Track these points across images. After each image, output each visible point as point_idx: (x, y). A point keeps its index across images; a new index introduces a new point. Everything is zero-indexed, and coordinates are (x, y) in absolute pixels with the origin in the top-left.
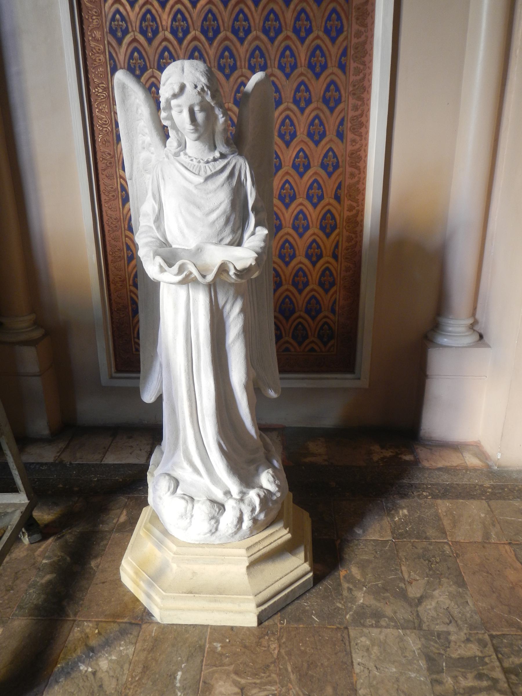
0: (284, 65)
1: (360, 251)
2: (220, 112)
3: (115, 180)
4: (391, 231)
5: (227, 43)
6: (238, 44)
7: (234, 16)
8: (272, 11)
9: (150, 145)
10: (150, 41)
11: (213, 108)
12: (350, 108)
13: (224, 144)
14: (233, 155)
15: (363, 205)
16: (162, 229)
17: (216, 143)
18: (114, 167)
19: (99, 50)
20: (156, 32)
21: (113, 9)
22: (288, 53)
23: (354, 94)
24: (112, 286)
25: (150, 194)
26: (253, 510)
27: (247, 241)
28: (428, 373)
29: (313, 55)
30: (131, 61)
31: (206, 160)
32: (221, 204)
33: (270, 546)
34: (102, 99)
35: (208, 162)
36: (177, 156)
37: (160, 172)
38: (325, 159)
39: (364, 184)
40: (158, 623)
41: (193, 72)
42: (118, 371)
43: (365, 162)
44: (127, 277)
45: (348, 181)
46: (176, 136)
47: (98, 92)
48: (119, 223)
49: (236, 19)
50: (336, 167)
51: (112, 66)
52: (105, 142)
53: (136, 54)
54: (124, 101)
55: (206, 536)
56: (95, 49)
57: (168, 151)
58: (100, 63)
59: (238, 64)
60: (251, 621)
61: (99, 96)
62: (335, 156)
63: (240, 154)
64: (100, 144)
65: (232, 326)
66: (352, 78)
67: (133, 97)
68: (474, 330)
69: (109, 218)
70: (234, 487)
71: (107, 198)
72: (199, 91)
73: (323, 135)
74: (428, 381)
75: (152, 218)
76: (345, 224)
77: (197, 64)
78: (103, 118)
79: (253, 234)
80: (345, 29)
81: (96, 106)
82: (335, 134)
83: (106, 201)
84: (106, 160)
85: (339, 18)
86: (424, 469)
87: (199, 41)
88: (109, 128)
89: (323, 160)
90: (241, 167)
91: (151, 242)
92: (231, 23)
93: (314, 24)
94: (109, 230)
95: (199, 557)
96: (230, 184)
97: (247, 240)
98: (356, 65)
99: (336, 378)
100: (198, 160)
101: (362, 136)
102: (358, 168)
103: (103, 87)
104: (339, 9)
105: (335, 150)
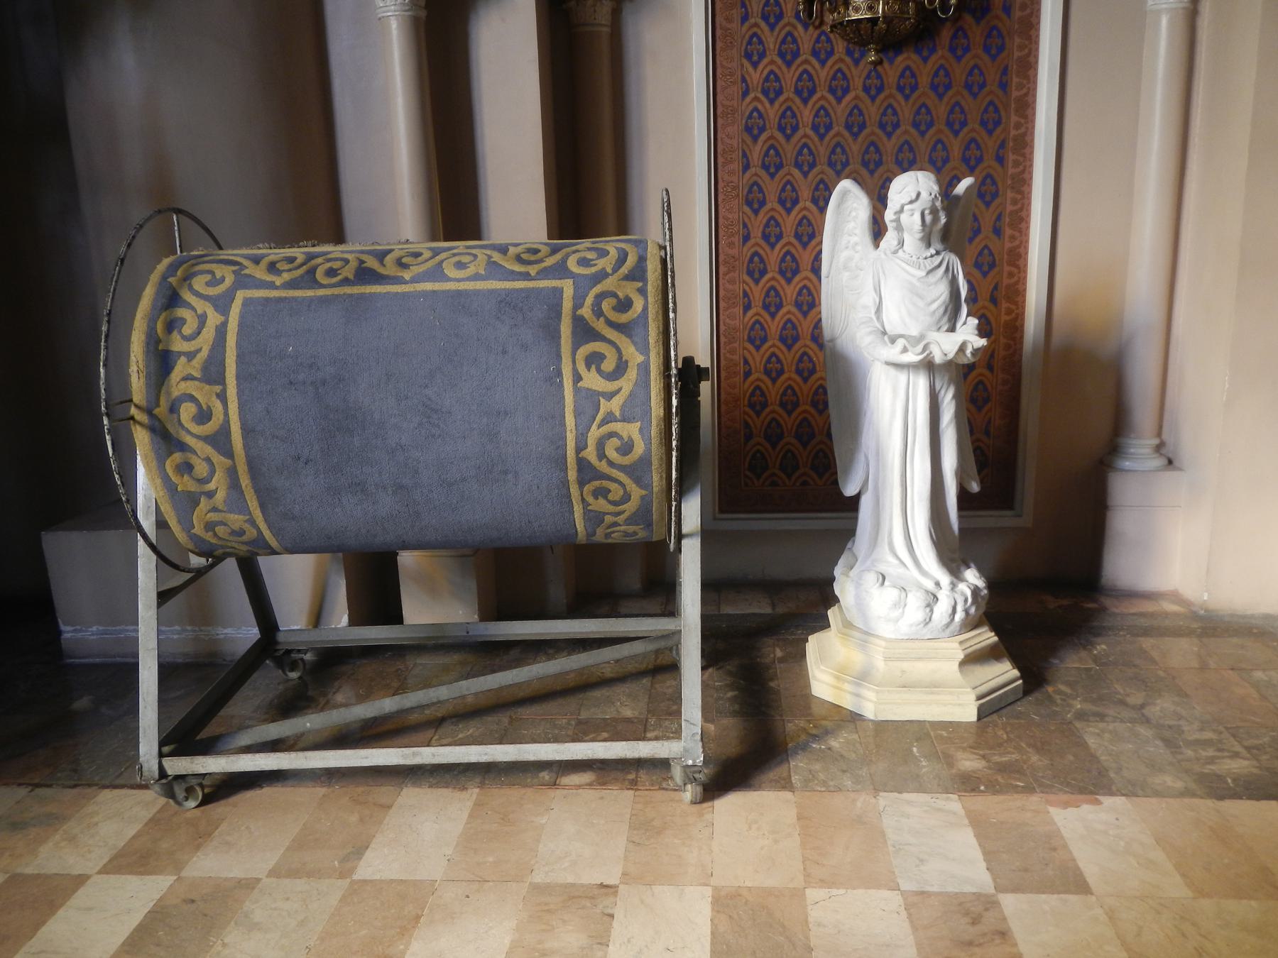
1: (1020, 360)
6: (885, 139)
7: (881, 111)
8: (924, 105)
9: (856, 244)
10: (788, 138)
12: (1008, 202)
15: (1024, 308)
17: (932, 241)
18: (737, 271)
21: (750, 108)
22: (939, 146)
23: (1013, 188)
24: (723, 408)
26: (966, 600)
28: (1110, 503)
29: (967, 148)
31: (924, 256)
33: (981, 640)
35: (926, 258)
39: (1025, 284)
40: (872, 721)
41: (927, 181)
42: (721, 511)
43: (1026, 260)
44: (742, 396)
45: (1006, 281)
48: (738, 334)
49: (884, 114)
50: (992, 265)
51: (744, 164)
55: (918, 628)
59: (884, 158)
62: (991, 254)
63: (950, 251)
65: (945, 412)
66: (1011, 171)
68: (1161, 454)
70: (945, 578)
74: (1110, 514)
75: (873, 311)
79: (965, 323)
80: (1004, 121)
82: (991, 230)
85: (997, 110)
87: (842, 136)
89: (977, 258)
92: (878, 119)
93: (969, 116)
95: (911, 651)
98: (1015, 157)
99: (991, 516)
102: (1018, 267)
104: (997, 102)
105: (991, 248)
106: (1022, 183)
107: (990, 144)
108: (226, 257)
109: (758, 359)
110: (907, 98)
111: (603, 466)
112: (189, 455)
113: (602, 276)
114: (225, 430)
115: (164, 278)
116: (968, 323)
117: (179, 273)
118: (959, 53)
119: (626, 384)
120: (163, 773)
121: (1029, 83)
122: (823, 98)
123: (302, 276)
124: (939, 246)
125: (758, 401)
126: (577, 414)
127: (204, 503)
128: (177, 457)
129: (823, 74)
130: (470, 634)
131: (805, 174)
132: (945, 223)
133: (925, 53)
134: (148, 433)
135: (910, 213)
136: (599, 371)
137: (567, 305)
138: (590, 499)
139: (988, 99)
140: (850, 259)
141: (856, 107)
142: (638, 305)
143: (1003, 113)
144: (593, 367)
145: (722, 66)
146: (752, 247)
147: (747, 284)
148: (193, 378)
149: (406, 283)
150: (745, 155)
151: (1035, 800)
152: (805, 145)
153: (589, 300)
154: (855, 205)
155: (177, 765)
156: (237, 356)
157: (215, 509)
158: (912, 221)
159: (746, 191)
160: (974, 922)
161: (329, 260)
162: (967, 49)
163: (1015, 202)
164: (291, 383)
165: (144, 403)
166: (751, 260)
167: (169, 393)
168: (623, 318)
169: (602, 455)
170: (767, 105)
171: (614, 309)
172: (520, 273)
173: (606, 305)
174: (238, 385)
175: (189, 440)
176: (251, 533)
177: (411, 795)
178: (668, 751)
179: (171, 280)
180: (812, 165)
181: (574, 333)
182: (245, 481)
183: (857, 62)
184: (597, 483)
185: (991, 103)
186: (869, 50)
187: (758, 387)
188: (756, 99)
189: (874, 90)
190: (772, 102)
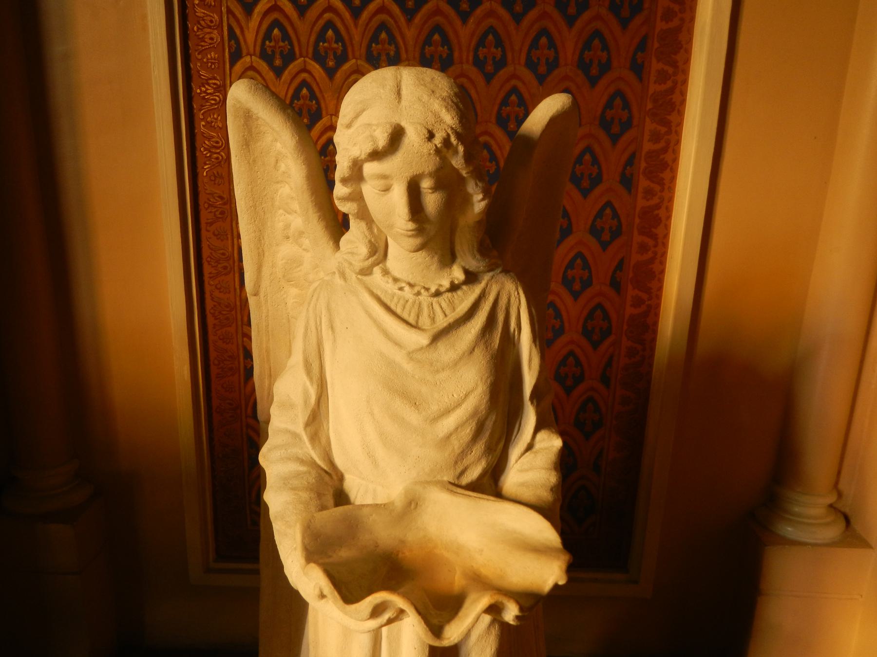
0: (536, 61)
2: (479, 190)
3: (230, 242)
4: (703, 344)
5: (438, 19)
6: (458, 22)
9: (301, 233)
11: (462, 180)
12: (646, 137)
13: (475, 252)
14: (491, 274)
15: (659, 297)
16: (323, 440)
17: (458, 247)
18: (229, 219)
19: (211, 21)
22: (544, 40)
25: (297, 358)
27: (517, 466)
30: (267, 43)
32: (467, 396)
34: (212, 104)
35: (438, 294)
36: (366, 275)
37: (324, 312)
38: (598, 220)
39: (663, 263)
41: (425, 98)
43: (667, 227)
44: (243, 402)
46: (367, 233)
47: (205, 92)
48: (233, 312)
50: (617, 233)
51: (233, 50)
52: (215, 177)
53: (276, 31)
54: (247, 144)
56: (204, 20)
57: (346, 265)
58: (211, 44)
59: (456, 54)
61: (207, 100)
62: (615, 215)
63: (506, 271)
64: (206, 180)
66: (653, 88)
67: (269, 138)
69: (215, 303)
71: (214, 271)
72: (439, 146)
73: (597, 180)
75: (302, 417)
76: (625, 327)
77: (432, 79)
78: (213, 137)
79: (530, 447)
81: (201, 117)
83: (212, 275)
84: (216, 207)
88: (222, 154)
89: (594, 221)
90: (509, 300)
91: (298, 475)
94: (215, 325)
96: (487, 345)
97: (516, 462)
100: (416, 289)
101: (664, 184)
102: (655, 237)
103: (215, 84)
116: (538, 446)
124: (474, 264)
132: (489, 211)
135: (381, 183)
163: (656, 137)
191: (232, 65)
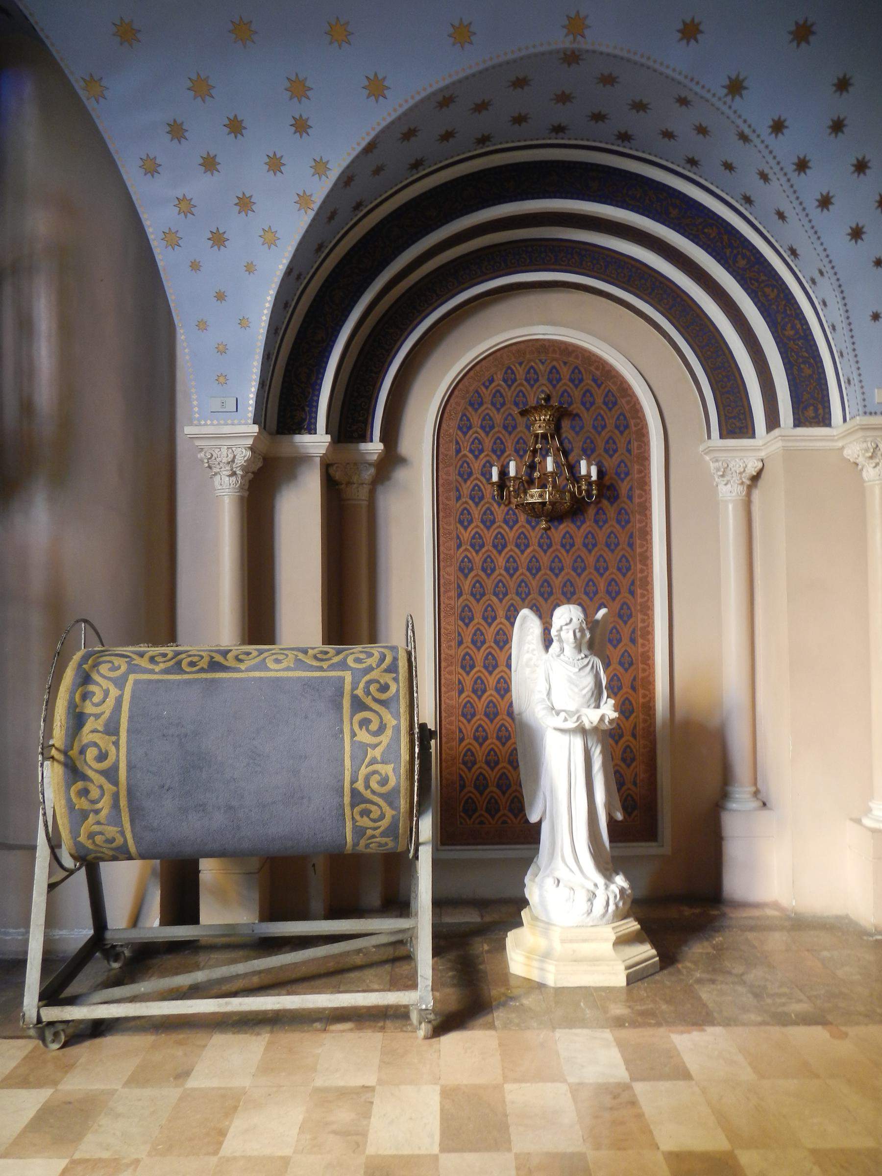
1: (655, 731)
6: (554, 577)
7: (551, 559)
8: (579, 556)
9: (534, 650)
10: (489, 576)
12: (639, 622)
15: (654, 693)
20: (493, 570)
21: (463, 555)
24: (444, 764)
26: (615, 897)
29: (609, 584)
39: (654, 677)
40: (553, 988)
43: (654, 660)
45: (641, 675)
49: (553, 561)
50: (631, 664)
53: (477, 584)
54: (522, 625)
59: (554, 591)
60: (623, 983)
62: (629, 655)
66: (639, 600)
70: (600, 880)
73: (619, 641)
75: (545, 693)
79: (606, 703)
80: (632, 567)
82: (628, 639)
85: (627, 561)
86: (731, 918)
87: (525, 575)
92: (549, 564)
93: (609, 564)
96: (593, 672)
98: (641, 591)
102: (648, 665)
104: (627, 554)
106: (647, 608)
107: (625, 582)
108: (120, 652)
109: (469, 728)
110: (568, 552)
111: (368, 794)
112: (89, 783)
113: (370, 669)
114: (115, 768)
115: (80, 665)
117: (90, 662)
118: (601, 523)
119: (385, 739)
120: (39, 1020)
121: (647, 543)
122: (511, 550)
123: (172, 666)
124: (587, 652)
125: (469, 761)
126: (352, 758)
127: (92, 818)
128: (80, 785)
129: (511, 535)
130: (255, 932)
131: (501, 600)
132: (590, 638)
133: (578, 523)
134: (63, 768)
136: (368, 730)
137: (347, 687)
138: (358, 817)
139: (621, 553)
140: (530, 659)
141: (534, 556)
142: (393, 688)
143: (632, 563)
144: (364, 727)
145: (444, 528)
146: (465, 648)
147: (461, 675)
148: (98, 731)
149: (242, 671)
150: (459, 586)
151: (662, 1031)
152: (500, 581)
153: (362, 685)
154: (532, 625)
155: (52, 1014)
156: (129, 717)
157: (98, 823)
158: (568, 636)
159: (460, 610)
160: (615, 1098)
161: (190, 656)
162: (605, 522)
163: (643, 621)
164: (164, 735)
165: (62, 747)
166: (464, 658)
167: (80, 741)
168: (383, 697)
169: (367, 786)
170: (474, 554)
171: (378, 690)
172: (317, 667)
173: (373, 688)
174: (128, 736)
175: (90, 773)
176: (119, 841)
177: (219, 1039)
178: (408, 1000)
179: (84, 666)
180: (505, 594)
181: (352, 705)
182: (123, 802)
183: (533, 528)
184: (363, 806)
185: (623, 556)
186: (542, 521)
187: (469, 750)
188: (466, 550)
189: (546, 546)
190: (477, 552)
191: (458, 599)
